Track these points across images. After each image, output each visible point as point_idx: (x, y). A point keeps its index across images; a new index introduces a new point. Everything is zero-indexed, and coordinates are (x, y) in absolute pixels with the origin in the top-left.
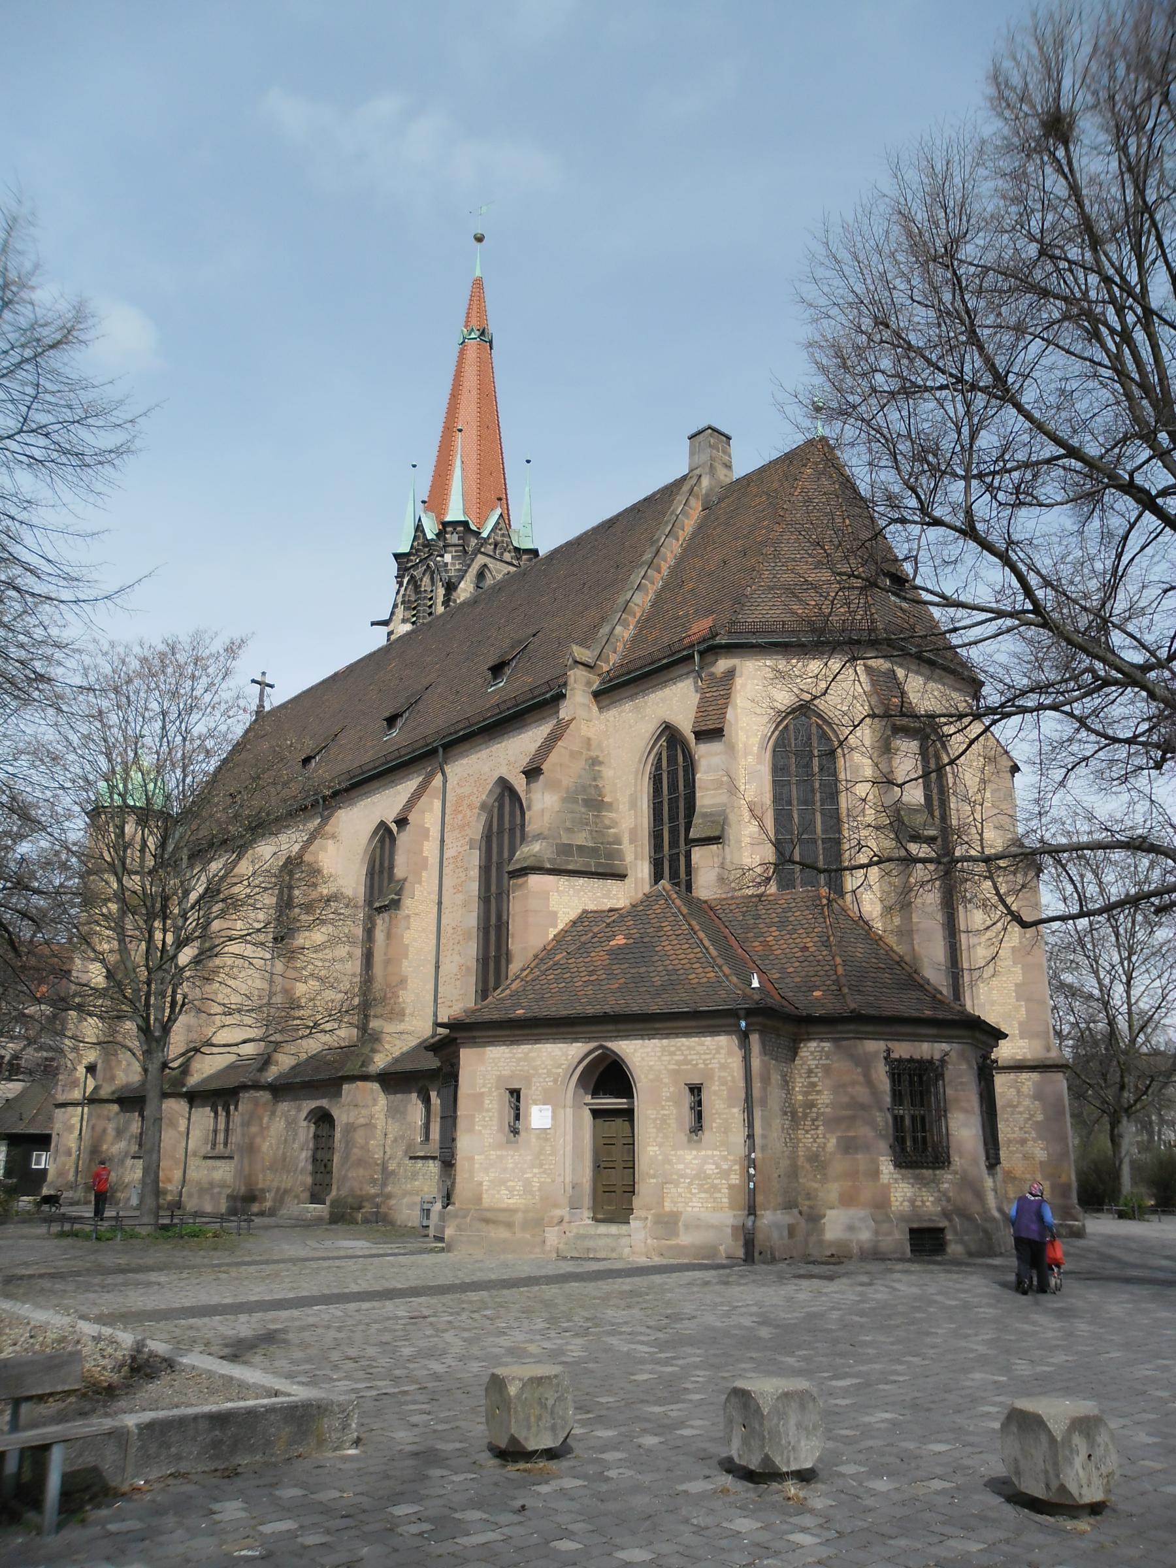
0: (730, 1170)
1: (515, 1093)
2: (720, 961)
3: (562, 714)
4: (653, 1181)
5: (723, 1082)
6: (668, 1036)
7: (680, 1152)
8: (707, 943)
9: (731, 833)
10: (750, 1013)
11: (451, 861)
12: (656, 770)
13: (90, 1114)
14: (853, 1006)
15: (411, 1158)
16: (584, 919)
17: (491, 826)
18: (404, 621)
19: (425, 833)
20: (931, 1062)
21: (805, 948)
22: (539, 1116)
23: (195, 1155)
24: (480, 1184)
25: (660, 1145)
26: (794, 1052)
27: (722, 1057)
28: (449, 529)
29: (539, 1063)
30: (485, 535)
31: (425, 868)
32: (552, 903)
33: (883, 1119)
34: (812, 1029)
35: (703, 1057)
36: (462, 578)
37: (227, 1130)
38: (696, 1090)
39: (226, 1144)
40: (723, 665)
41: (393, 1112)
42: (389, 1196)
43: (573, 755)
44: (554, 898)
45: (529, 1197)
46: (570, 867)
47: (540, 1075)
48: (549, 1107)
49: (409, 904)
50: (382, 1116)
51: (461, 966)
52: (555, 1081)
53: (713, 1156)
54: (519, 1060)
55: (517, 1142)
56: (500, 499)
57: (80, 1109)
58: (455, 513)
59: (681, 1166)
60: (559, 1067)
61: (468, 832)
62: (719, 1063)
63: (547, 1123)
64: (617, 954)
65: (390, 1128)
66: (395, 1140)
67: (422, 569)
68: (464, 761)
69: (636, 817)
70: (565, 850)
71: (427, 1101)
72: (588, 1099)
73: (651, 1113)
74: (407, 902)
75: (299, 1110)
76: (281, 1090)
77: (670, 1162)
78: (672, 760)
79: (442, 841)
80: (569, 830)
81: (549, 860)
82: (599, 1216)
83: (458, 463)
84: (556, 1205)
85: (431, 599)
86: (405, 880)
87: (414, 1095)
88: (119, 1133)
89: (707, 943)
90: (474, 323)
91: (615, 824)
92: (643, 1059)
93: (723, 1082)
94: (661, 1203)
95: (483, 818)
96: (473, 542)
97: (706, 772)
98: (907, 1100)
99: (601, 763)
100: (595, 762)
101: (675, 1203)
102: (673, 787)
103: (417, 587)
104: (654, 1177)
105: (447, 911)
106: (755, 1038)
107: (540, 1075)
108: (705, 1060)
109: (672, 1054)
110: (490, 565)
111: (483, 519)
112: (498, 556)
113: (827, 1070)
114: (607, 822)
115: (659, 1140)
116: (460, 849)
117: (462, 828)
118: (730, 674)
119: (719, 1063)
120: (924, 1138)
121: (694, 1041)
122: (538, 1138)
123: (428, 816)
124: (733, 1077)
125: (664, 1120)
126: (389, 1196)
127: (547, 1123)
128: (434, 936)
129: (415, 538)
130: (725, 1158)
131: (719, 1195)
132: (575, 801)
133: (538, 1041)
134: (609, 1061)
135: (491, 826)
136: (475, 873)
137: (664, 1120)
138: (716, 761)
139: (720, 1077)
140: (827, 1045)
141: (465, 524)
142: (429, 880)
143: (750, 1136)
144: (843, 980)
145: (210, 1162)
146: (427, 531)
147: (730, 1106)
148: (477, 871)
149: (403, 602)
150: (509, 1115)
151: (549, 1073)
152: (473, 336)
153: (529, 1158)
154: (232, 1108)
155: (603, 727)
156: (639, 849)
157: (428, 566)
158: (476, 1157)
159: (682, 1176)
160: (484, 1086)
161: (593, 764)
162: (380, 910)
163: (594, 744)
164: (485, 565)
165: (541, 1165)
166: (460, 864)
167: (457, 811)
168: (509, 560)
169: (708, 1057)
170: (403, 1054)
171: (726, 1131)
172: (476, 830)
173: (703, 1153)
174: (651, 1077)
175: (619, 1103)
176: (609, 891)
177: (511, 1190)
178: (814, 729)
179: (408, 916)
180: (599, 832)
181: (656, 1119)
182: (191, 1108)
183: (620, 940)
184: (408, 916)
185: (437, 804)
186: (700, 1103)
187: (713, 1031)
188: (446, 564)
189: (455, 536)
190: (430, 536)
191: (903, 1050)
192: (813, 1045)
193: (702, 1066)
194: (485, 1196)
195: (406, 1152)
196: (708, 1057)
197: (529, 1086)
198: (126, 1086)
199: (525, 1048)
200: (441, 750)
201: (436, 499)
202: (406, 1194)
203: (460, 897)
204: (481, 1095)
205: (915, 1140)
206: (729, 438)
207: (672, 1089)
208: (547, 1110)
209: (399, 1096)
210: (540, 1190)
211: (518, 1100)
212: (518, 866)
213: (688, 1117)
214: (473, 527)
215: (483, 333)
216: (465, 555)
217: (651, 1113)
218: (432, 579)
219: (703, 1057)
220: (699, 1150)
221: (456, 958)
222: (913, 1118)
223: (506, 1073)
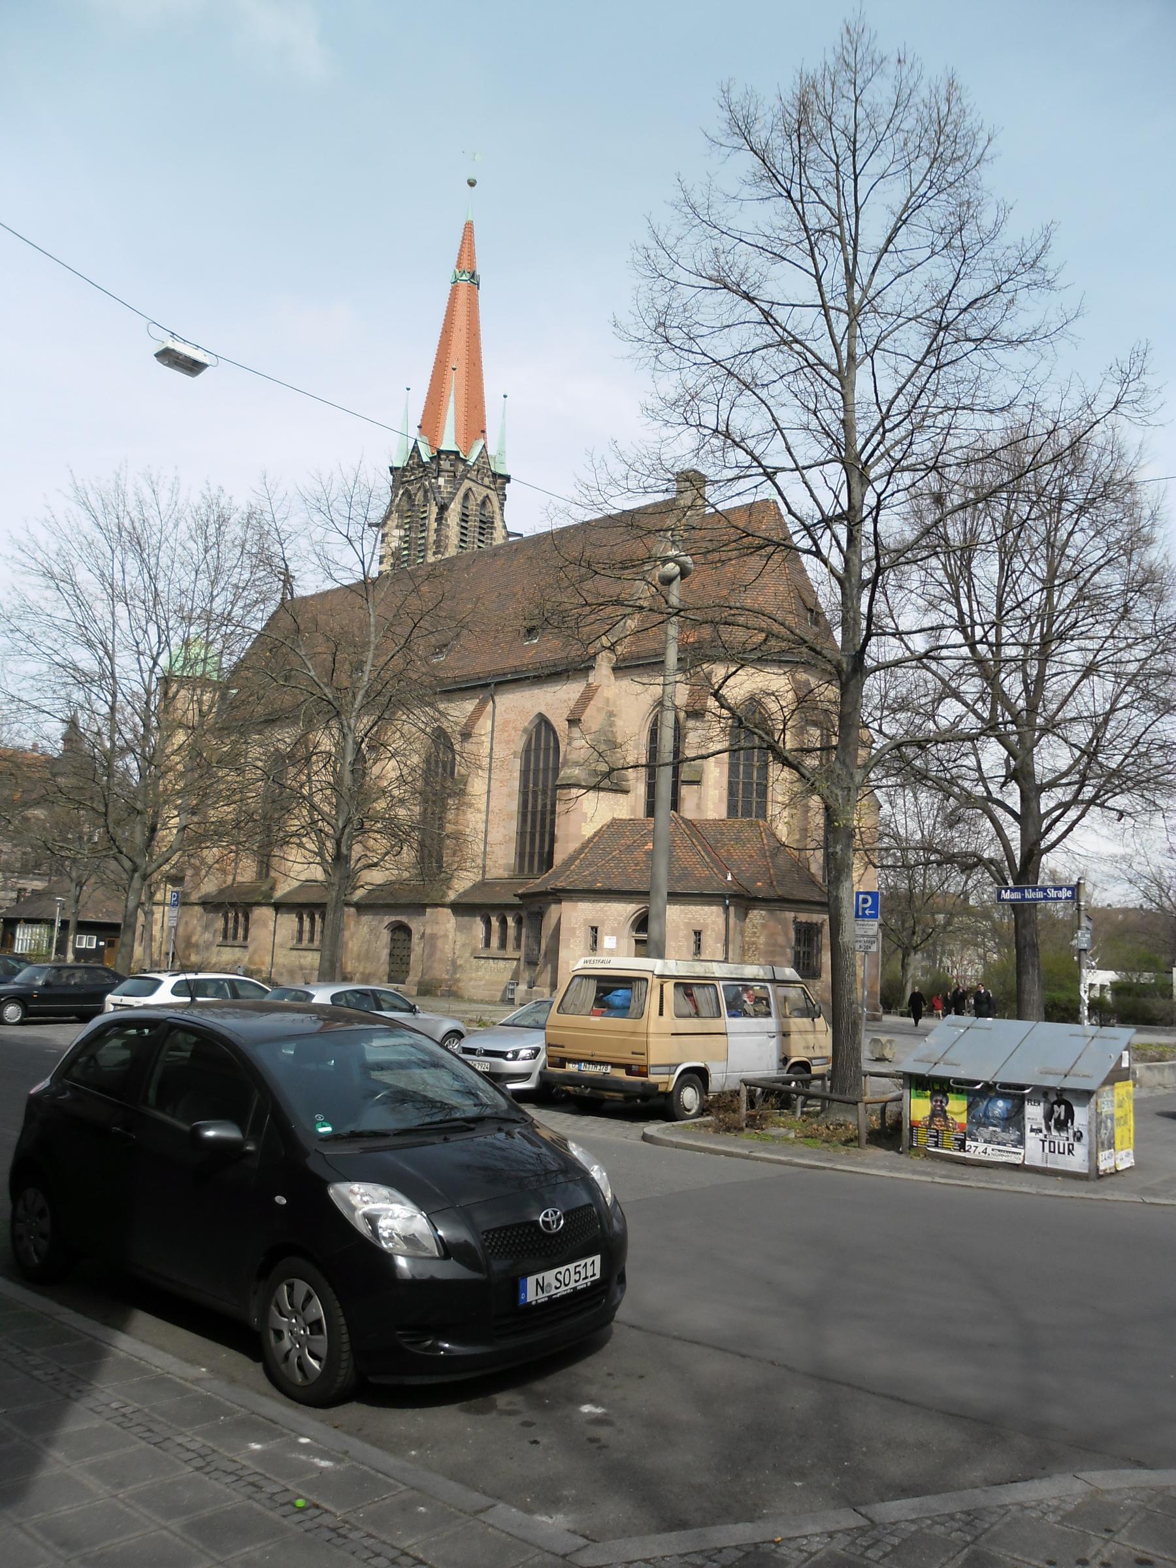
1: (595, 929)
2: (711, 865)
3: (591, 680)
5: (713, 930)
6: (684, 904)
8: (703, 853)
9: (704, 780)
10: (731, 896)
12: (653, 725)
13: (169, 911)
14: (780, 893)
18: (397, 527)
20: (816, 924)
21: (751, 857)
23: (281, 946)
26: (746, 915)
27: (713, 918)
28: (443, 456)
33: (790, 953)
34: (757, 904)
36: (452, 499)
38: (698, 934)
41: (459, 928)
42: (458, 980)
43: (599, 710)
50: (452, 930)
51: (505, 836)
52: (619, 924)
54: (597, 911)
57: (162, 907)
61: (513, 746)
65: (458, 938)
66: (464, 945)
68: (511, 696)
71: (488, 923)
72: (634, 934)
73: (673, 944)
75: (381, 921)
81: (584, 780)
83: (452, 398)
87: (478, 919)
88: (206, 927)
89: (703, 853)
90: (465, 265)
93: (713, 930)
95: (525, 738)
96: (461, 467)
98: (802, 944)
99: (615, 716)
100: (611, 714)
106: (732, 909)
109: (686, 914)
110: (474, 489)
111: (468, 447)
112: (480, 482)
113: (764, 926)
117: (507, 742)
120: (808, 964)
126: (458, 980)
129: (411, 457)
133: (609, 902)
136: (517, 774)
140: (763, 912)
141: (457, 453)
144: (773, 878)
145: (295, 952)
147: (717, 943)
148: (518, 773)
151: (615, 920)
155: (617, 691)
157: (423, 484)
161: (610, 716)
163: (611, 702)
164: (470, 489)
168: (487, 484)
170: (465, 891)
172: (519, 744)
176: (618, 801)
182: (277, 914)
186: (699, 940)
187: (710, 904)
189: (448, 463)
190: (425, 459)
191: (803, 917)
192: (755, 912)
195: (472, 954)
198: (206, 895)
199: (602, 905)
200: (493, 685)
201: (430, 423)
202: (471, 979)
203: (505, 790)
205: (804, 964)
209: (466, 918)
211: (596, 932)
213: (693, 947)
214: (462, 456)
215: (473, 276)
216: (455, 480)
217: (673, 944)
218: (425, 496)
222: (804, 953)
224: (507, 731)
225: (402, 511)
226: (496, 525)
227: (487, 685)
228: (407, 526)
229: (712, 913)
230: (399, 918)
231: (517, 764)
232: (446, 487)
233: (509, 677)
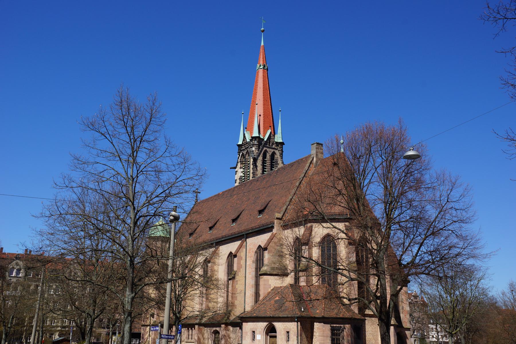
1: (254, 332)
10: (297, 318)
16: (275, 289)
17: (258, 258)
18: (241, 168)
19: (241, 258)
22: (258, 337)
30: (265, 140)
31: (241, 268)
37: (192, 335)
38: (288, 332)
39: (192, 339)
40: (309, 225)
44: (270, 281)
49: (237, 278)
52: (262, 330)
56: (270, 127)
58: (256, 134)
63: (260, 339)
64: (276, 301)
70: (273, 269)
73: (280, 337)
74: (237, 277)
76: (206, 325)
79: (246, 260)
81: (269, 272)
85: (249, 161)
95: (256, 255)
103: (244, 157)
109: (284, 325)
117: (251, 257)
118: (312, 226)
121: (288, 323)
123: (242, 254)
127: (260, 339)
129: (243, 140)
134: (272, 326)
135: (258, 258)
136: (254, 270)
137: (282, 338)
141: (259, 137)
142: (242, 270)
146: (247, 138)
147: (294, 336)
148: (254, 269)
149: (240, 162)
151: (260, 328)
152: (261, 67)
154: (193, 329)
162: (230, 279)
164: (266, 150)
166: (250, 267)
171: (293, 341)
179: (237, 281)
183: (277, 298)
184: (237, 281)
185: (244, 250)
186: (289, 335)
188: (253, 151)
190: (248, 140)
197: (256, 331)
204: (247, 332)
206: (322, 145)
212: (261, 273)
217: (280, 337)
224: (250, 253)
225: (243, 161)
226: (279, 163)
227: (243, 235)
228: (244, 167)
230: (214, 329)
231: (254, 266)
232: (256, 151)
233: (250, 231)
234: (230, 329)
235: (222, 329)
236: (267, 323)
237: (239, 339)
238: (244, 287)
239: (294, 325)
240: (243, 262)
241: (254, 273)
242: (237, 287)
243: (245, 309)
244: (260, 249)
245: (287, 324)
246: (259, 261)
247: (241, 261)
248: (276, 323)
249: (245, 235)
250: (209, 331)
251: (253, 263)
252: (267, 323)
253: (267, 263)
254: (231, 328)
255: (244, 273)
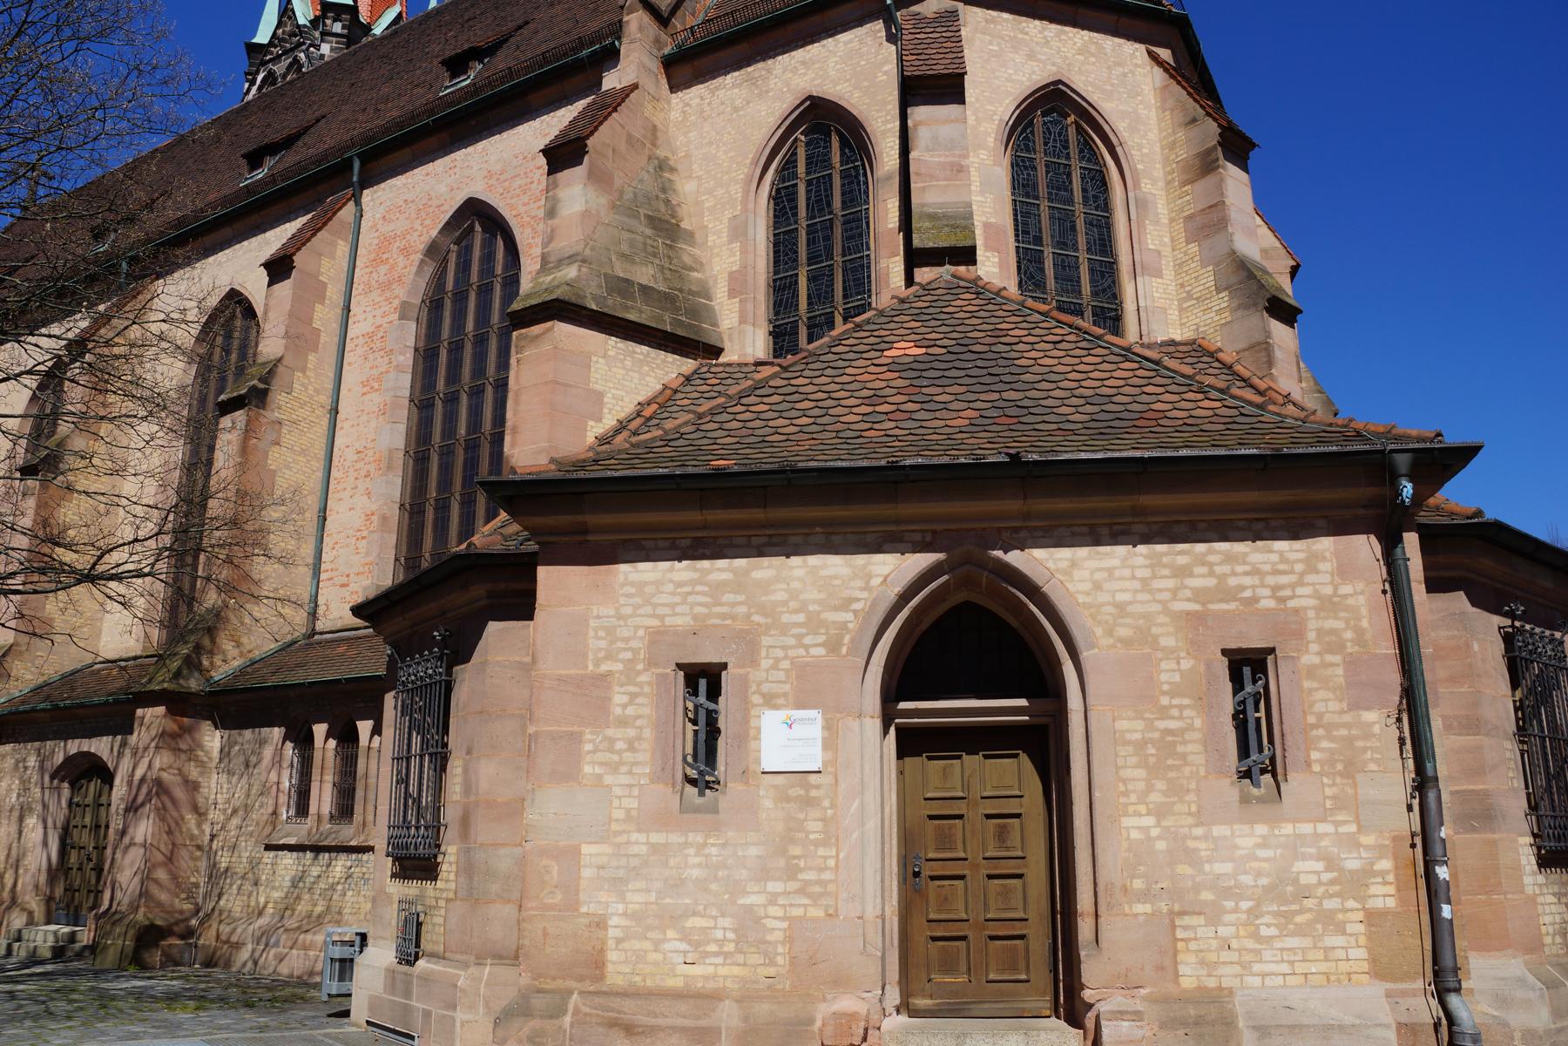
0: (1368, 872)
4: (1140, 908)
5: (1333, 644)
7: (1219, 830)
11: (361, 341)
15: (268, 848)
19: (320, 292)
24: (600, 923)
25: (1160, 813)
27: (1323, 580)
29: (780, 596)
30: (378, 30)
32: (594, 375)
35: (1271, 580)
44: (599, 368)
45: (756, 959)
46: (632, 316)
47: (784, 629)
48: (813, 713)
51: (368, 516)
52: (833, 646)
53: (1318, 837)
55: (714, 810)
59: (1226, 868)
60: (845, 605)
62: (1317, 595)
67: (285, 62)
69: (744, 252)
70: (623, 287)
71: (303, 741)
73: (1132, 727)
74: (278, 398)
77: (1191, 857)
78: (818, 160)
79: (347, 309)
80: (624, 257)
81: (595, 298)
82: (921, 1002)
84: (841, 982)
86: (280, 360)
91: (699, 265)
92: (1097, 586)
93: (1333, 644)
94: (1168, 966)
95: (429, 270)
97: (928, 150)
99: (672, 170)
101: (1211, 966)
102: (819, 202)
104: (1145, 896)
105: (346, 425)
107: (784, 629)
108: (1276, 588)
109: (1183, 572)
111: (376, 15)
114: (687, 259)
115: (1155, 797)
116: (378, 321)
117: (385, 286)
119: (1317, 595)
122: (783, 797)
124: (1359, 632)
125: (1168, 744)
128: (318, 465)
130: (1352, 843)
131: (1338, 941)
132: (636, 216)
136: (407, 359)
137: (1168, 744)
138: (946, 131)
139: (1319, 631)
143: (1423, 782)
146: (298, 14)
147: (1355, 706)
150: (685, 737)
153: (753, 851)
156: (750, 306)
157: (296, 60)
158: (586, 849)
159: (1227, 893)
160: (610, 656)
162: (227, 408)
165: (792, 872)
167: (377, 261)
169: (1284, 580)
171: (1351, 769)
173: (1288, 829)
174: (1124, 632)
175: (1011, 707)
177: (697, 941)
178: (1072, 131)
180: (677, 272)
181: (1142, 744)
185: (343, 248)
190: (302, 21)
193: (1270, 603)
194: (612, 956)
196: (1284, 580)
204: (603, 679)
207: (1186, 664)
208: (811, 724)
210: (790, 939)
211: (714, 692)
219: (1271, 580)
220: (1274, 822)
221: (361, 501)
223: (681, 621)
229: (1311, 565)
231: (409, 335)
234: (200, 746)
235: (138, 737)
236: (920, 561)
237: (275, 813)
238: (320, 475)
239: (1344, 571)
240: (325, 317)
241: (406, 380)
242: (272, 464)
243: (313, 615)
244: (471, 229)
245: (1229, 559)
246: (448, 304)
247: (318, 307)
248: (1064, 553)
249: (357, 164)
250: (32, 761)
251: (402, 317)
252: (920, 561)
253: (579, 248)
254: (212, 739)
255: (330, 386)
